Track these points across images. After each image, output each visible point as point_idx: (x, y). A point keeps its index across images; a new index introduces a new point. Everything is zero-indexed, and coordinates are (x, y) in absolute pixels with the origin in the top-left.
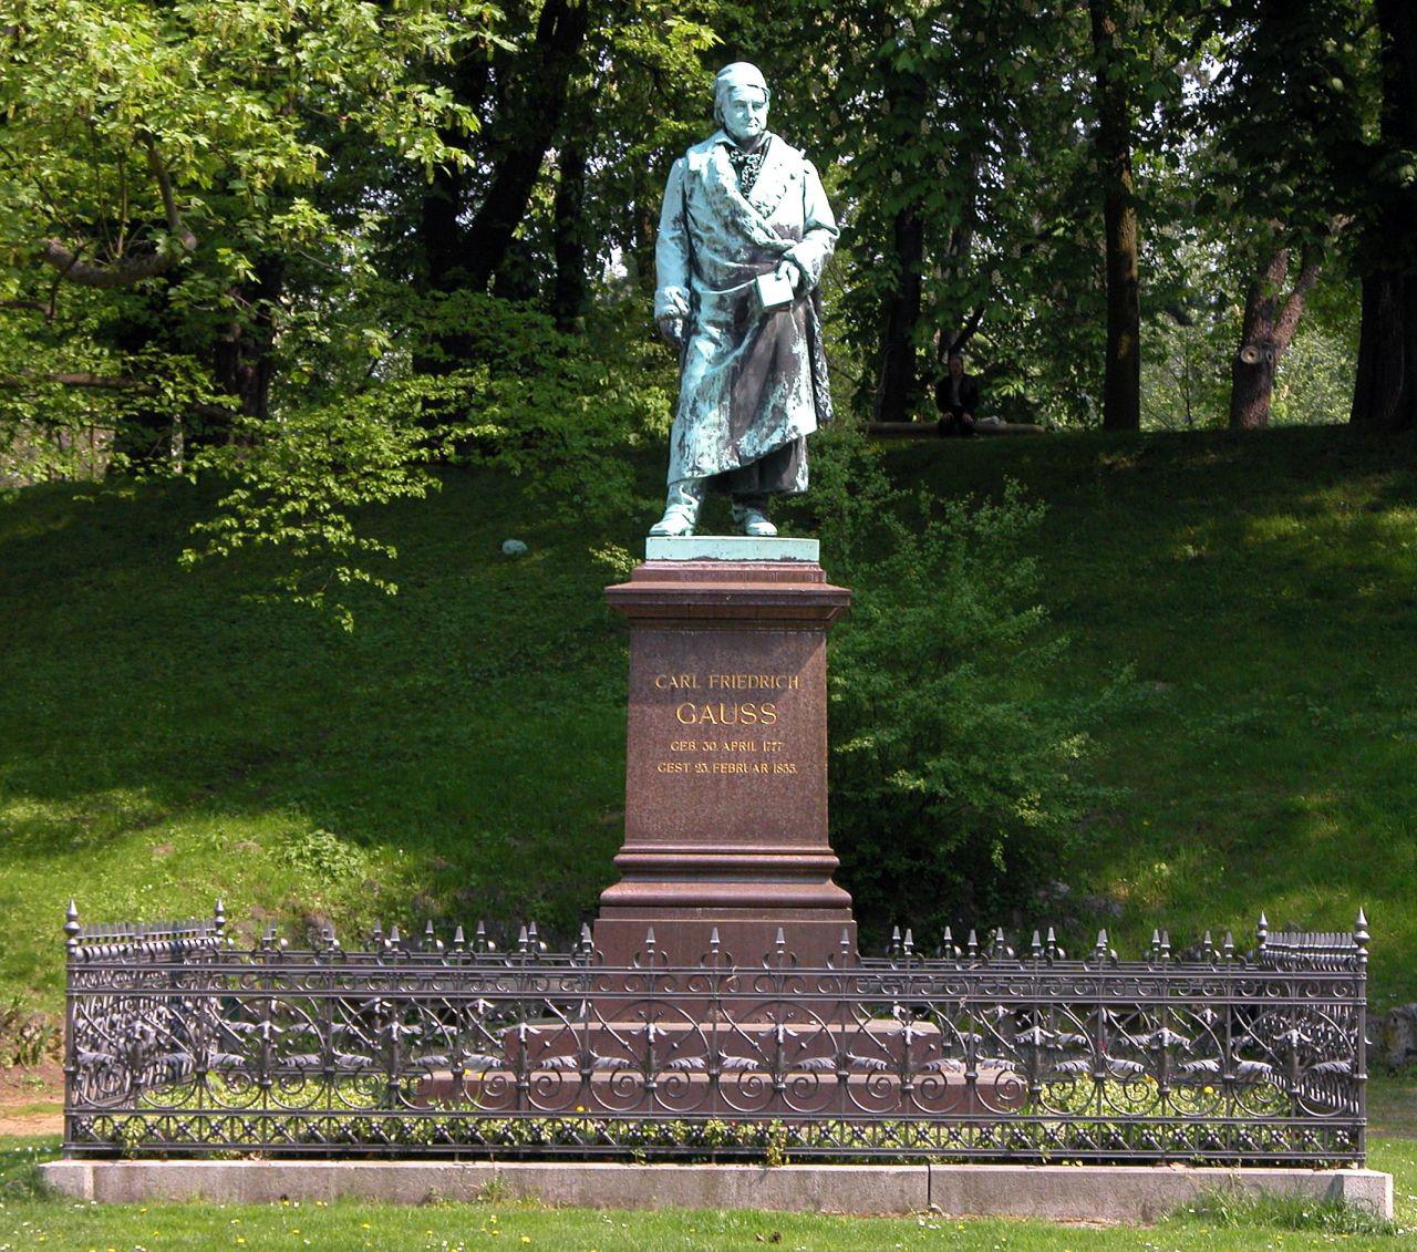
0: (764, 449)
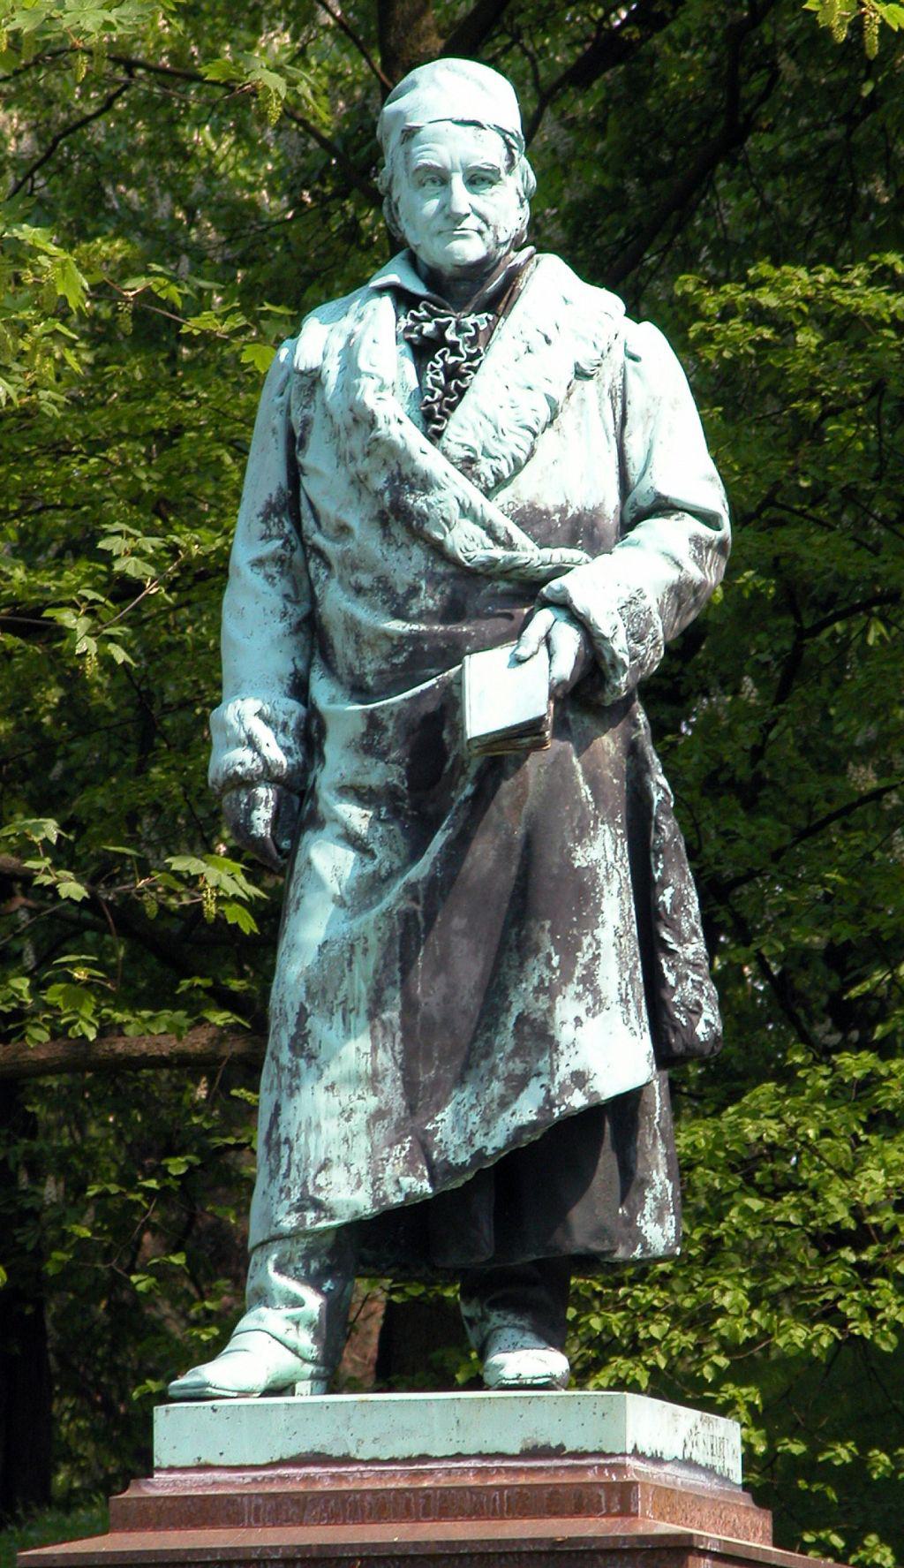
0: (496, 1140)
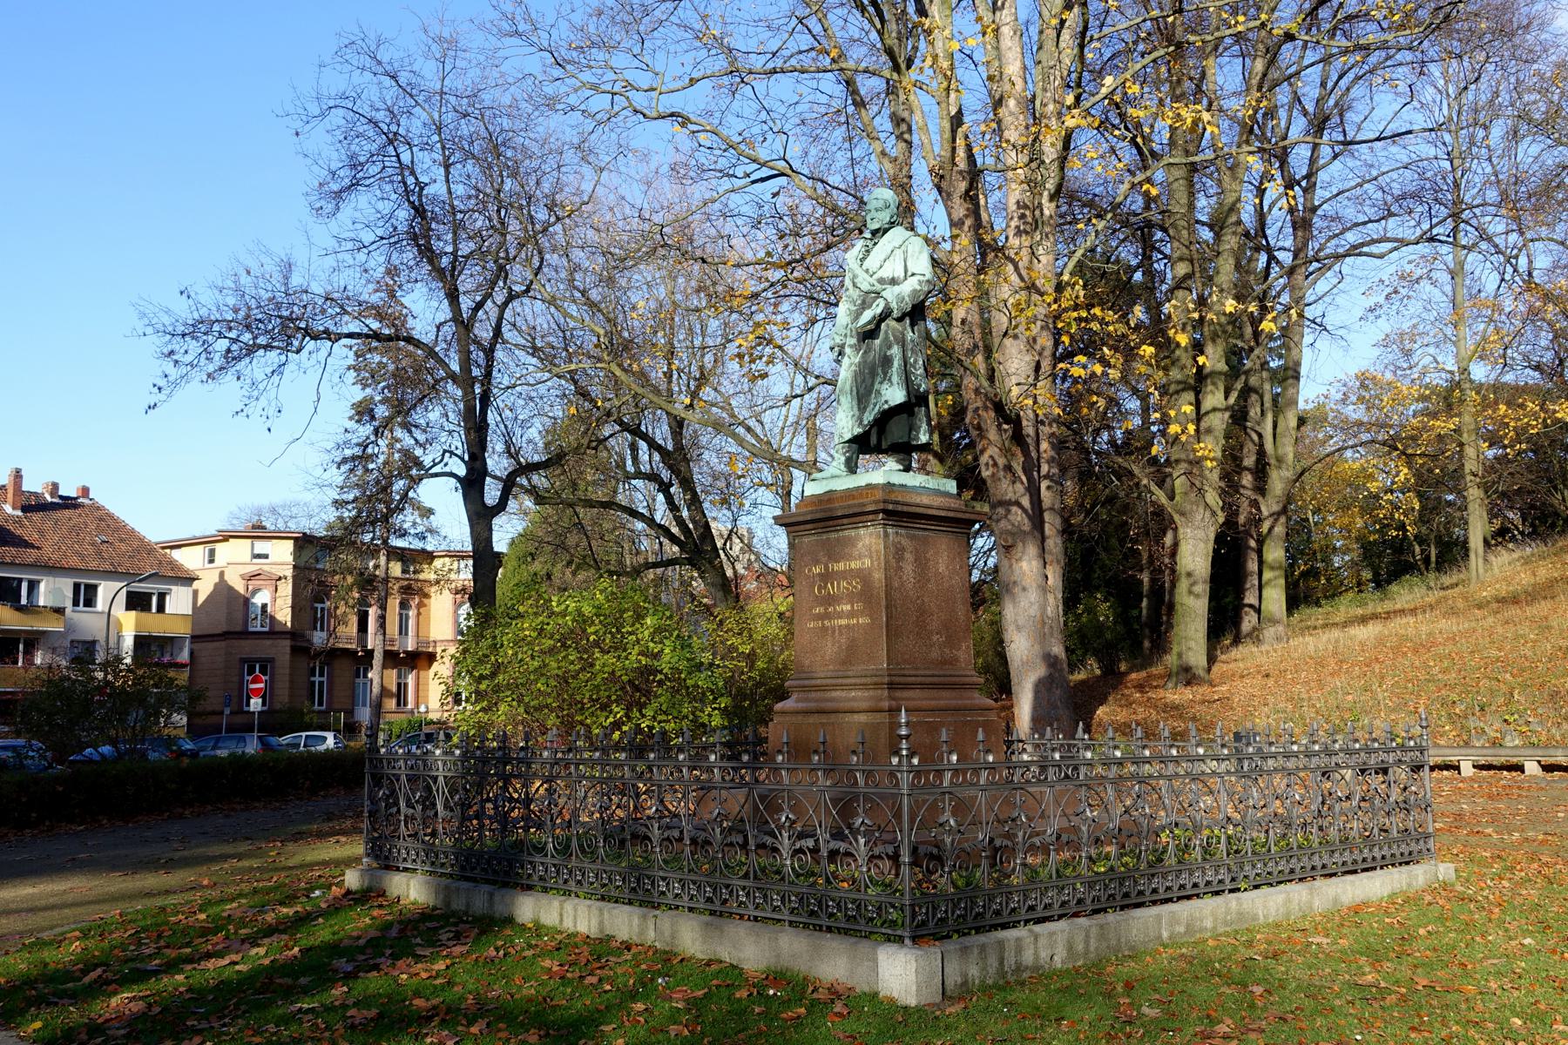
0: (871, 418)
